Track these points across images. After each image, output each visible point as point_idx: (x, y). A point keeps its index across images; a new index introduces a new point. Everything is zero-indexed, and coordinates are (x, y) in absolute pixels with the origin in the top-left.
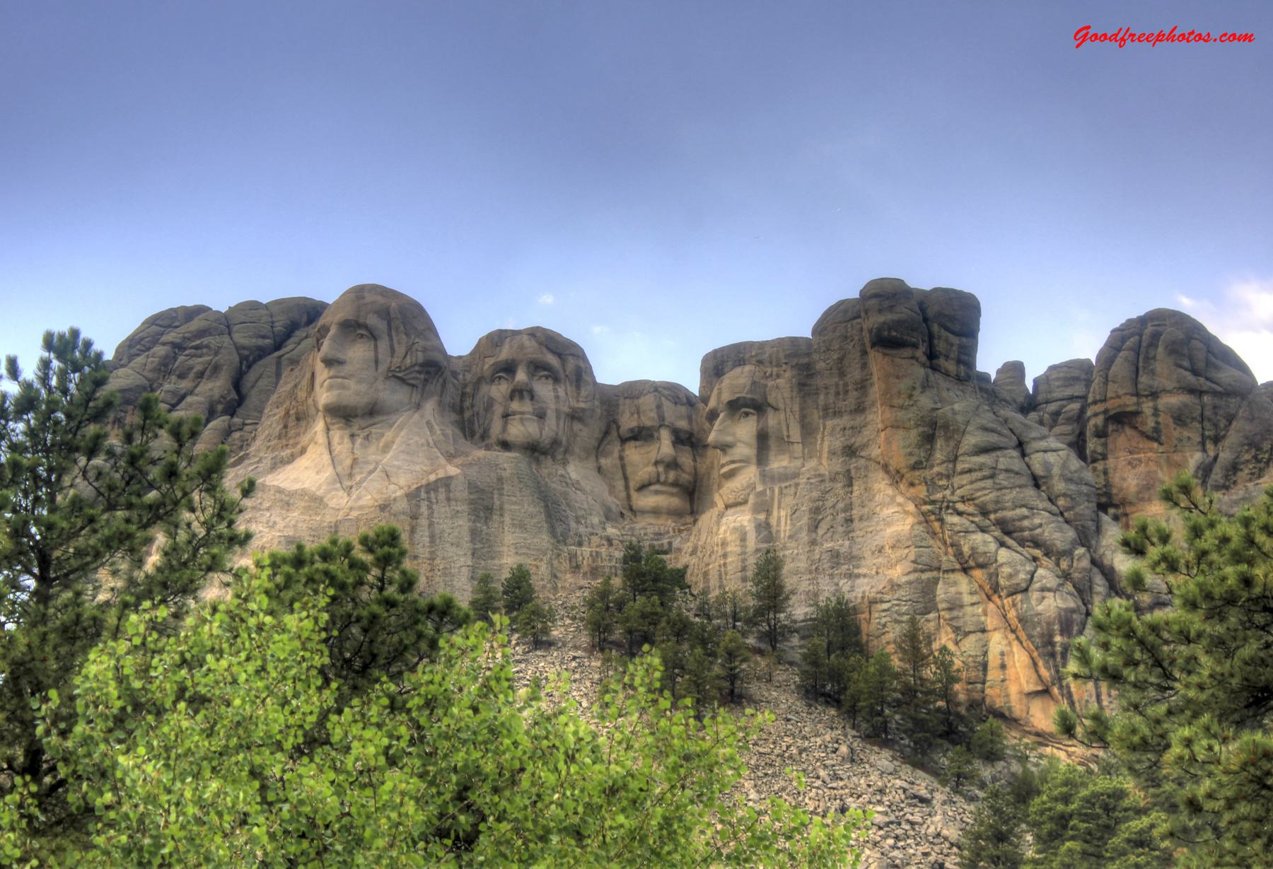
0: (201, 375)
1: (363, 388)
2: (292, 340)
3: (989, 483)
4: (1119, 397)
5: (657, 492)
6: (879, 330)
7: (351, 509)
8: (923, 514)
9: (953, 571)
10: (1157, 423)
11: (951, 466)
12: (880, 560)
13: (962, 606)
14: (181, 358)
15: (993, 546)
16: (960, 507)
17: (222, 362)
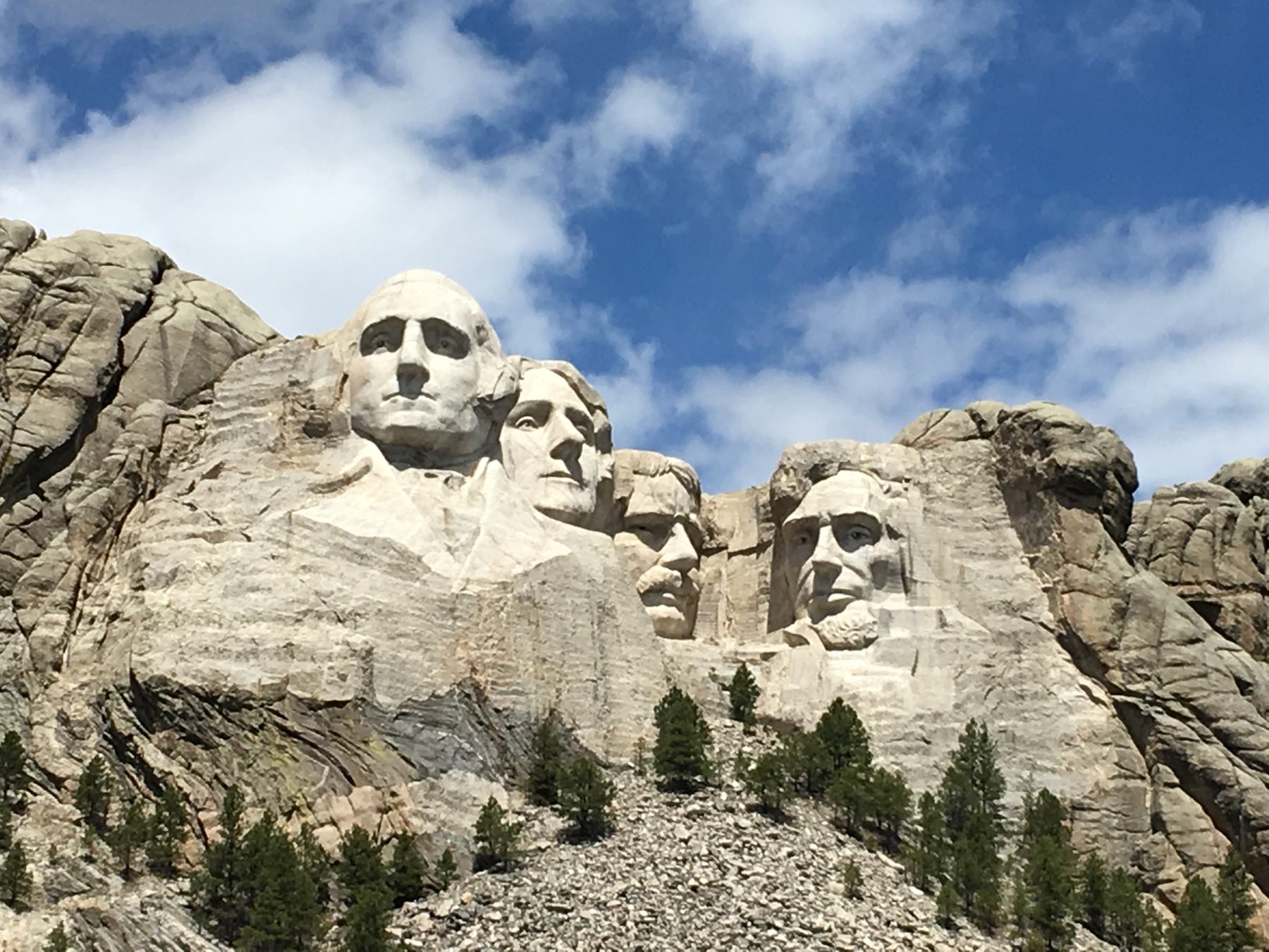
0: (77, 328)
1: (451, 414)
2: (157, 301)
3: (1200, 682)
4: (1199, 584)
5: (669, 603)
6: (1075, 468)
7: (468, 581)
8: (1116, 703)
9: (1173, 786)
10: (1237, 621)
11: (1153, 652)
12: (1071, 754)
13: (1192, 831)
14: (47, 301)
15: (1226, 765)
16: (1176, 706)
17: (105, 315)
